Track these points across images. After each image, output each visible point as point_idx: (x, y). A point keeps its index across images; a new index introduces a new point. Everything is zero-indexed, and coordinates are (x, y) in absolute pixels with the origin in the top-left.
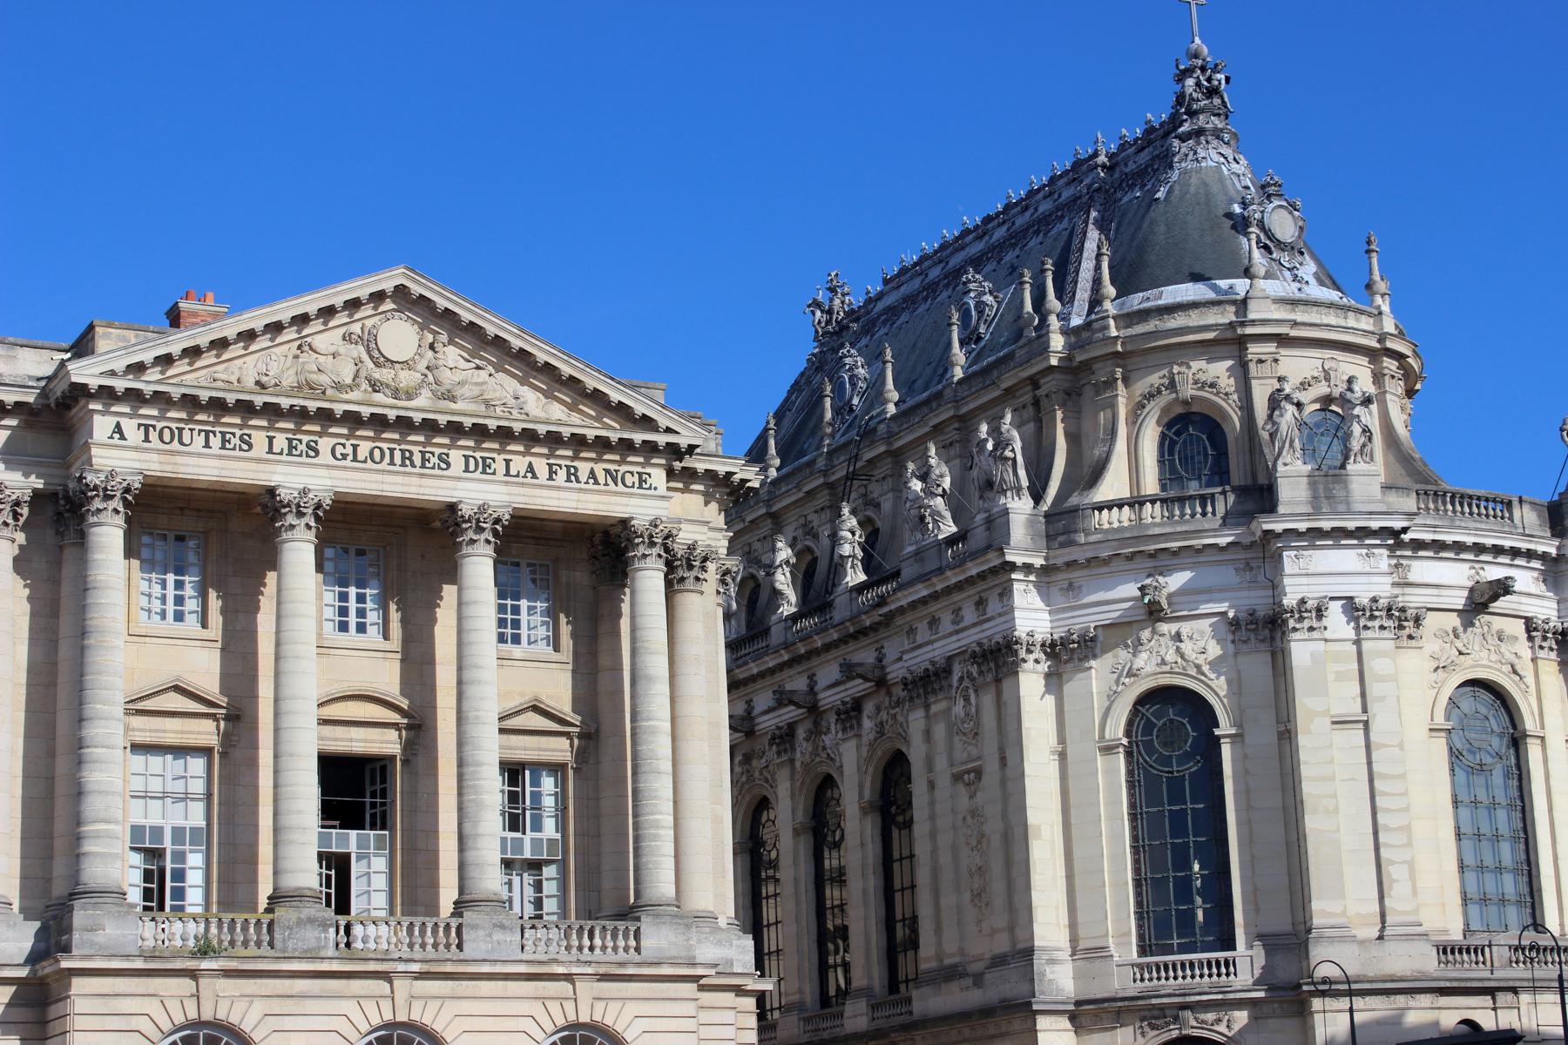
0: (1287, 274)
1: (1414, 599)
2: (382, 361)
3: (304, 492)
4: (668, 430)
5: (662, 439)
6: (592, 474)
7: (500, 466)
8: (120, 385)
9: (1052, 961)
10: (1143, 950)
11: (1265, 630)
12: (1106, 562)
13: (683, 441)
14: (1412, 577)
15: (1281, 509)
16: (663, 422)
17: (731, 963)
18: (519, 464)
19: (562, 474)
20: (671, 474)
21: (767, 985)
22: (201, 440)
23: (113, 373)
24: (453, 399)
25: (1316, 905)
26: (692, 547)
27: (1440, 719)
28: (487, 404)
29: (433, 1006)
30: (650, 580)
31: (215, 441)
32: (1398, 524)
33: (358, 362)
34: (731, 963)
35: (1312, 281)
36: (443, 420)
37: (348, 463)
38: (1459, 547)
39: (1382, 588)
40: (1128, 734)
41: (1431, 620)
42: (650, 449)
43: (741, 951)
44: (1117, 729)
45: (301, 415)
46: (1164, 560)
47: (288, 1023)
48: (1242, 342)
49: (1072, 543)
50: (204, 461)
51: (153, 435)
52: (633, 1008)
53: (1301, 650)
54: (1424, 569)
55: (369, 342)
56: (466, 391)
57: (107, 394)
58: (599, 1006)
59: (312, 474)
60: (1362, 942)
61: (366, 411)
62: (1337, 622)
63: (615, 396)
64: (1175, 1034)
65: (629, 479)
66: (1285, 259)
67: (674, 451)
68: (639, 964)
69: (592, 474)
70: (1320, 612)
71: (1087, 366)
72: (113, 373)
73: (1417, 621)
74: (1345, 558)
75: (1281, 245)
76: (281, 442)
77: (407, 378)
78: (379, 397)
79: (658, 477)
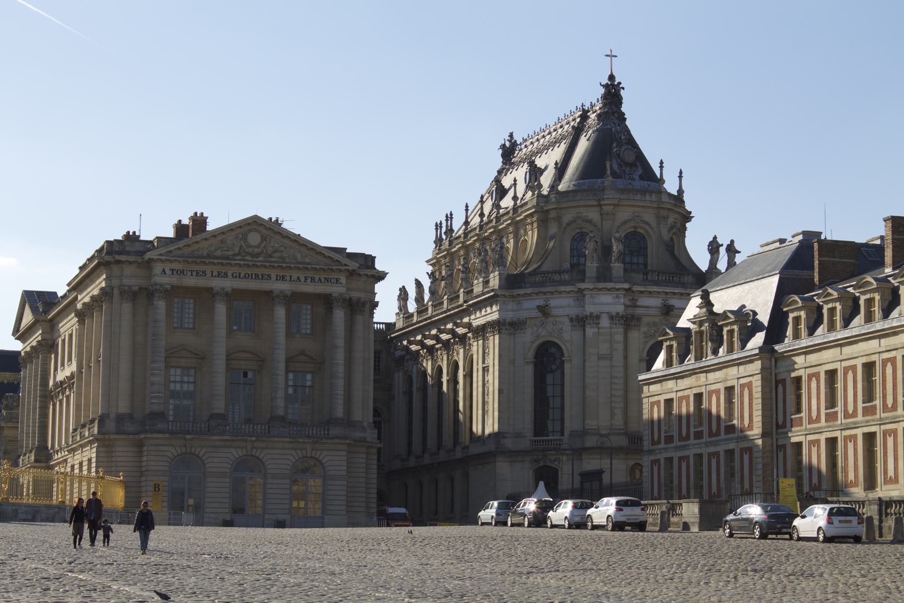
0: (627, 176)
1: (639, 311)
2: (249, 246)
3: (223, 289)
4: (345, 265)
5: (343, 268)
6: (320, 279)
7: (288, 278)
8: (163, 258)
9: (505, 437)
10: (535, 435)
11: (580, 322)
12: (530, 295)
13: (350, 268)
14: (638, 304)
15: (586, 280)
16: (343, 262)
17: (365, 438)
18: (295, 277)
19: (309, 280)
20: (347, 278)
21: (381, 445)
22: (189, 273)
23: (161, 255)
24: (272, 257)
25: (587, 422)
26: (359, 299)
27: (645, 354)
28: (283, 258)
29: (259, 451)
30: (339, 315)
31: (194, 274)
32: (626, 286)
33: (241, 247)
34: (365, 438)
35: (637, 178)
36: (267, 264)
37: (237, 279)
38: (659, 293)
39: (620, 309)
40: (536, 357)
41: (645, 320)
42: (340, 270)
43: (371, 435)
44: (531, 355)
45: (222, 264)
46: (549, 296)
47: (214, 455)
48: (600, 206)
49: (520, 287)
50: (191, 281)
51: (175, 272)
52: (325, 453)
53: (590, 331)
54: (644, 301)
55: (244, 238)
56: (277, 255)
57: (161, 260)
58: (314, 452)
59: (227, 284)
60: (602, 436)
61: (242, 263)
62: (605, 322)
63: (327, 254)
64: (542, 464)
65: (333, 281)
66: (627, 170)
67: (348, 270)
68: (327, 439)
69: (320, 279)
70: (598, 317)
71: (548, 211)
72: (161, 255)
73: (639, 319)
74: (607, 298)
75: (627, 164)
76: (215, 273)
77: (257, 250)
78: (247, 258)
79: (343, 280)
